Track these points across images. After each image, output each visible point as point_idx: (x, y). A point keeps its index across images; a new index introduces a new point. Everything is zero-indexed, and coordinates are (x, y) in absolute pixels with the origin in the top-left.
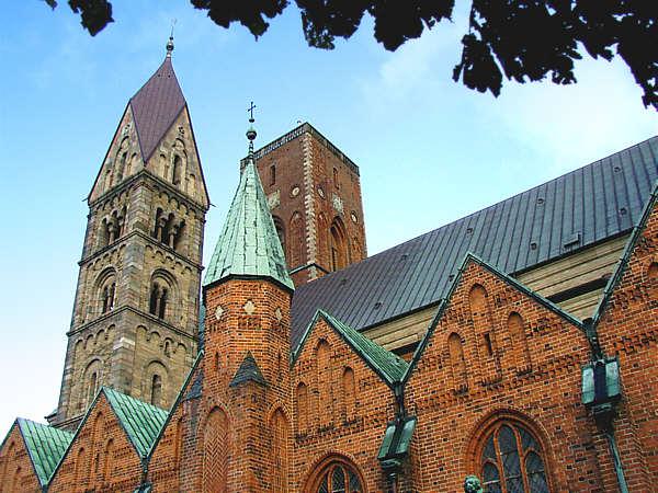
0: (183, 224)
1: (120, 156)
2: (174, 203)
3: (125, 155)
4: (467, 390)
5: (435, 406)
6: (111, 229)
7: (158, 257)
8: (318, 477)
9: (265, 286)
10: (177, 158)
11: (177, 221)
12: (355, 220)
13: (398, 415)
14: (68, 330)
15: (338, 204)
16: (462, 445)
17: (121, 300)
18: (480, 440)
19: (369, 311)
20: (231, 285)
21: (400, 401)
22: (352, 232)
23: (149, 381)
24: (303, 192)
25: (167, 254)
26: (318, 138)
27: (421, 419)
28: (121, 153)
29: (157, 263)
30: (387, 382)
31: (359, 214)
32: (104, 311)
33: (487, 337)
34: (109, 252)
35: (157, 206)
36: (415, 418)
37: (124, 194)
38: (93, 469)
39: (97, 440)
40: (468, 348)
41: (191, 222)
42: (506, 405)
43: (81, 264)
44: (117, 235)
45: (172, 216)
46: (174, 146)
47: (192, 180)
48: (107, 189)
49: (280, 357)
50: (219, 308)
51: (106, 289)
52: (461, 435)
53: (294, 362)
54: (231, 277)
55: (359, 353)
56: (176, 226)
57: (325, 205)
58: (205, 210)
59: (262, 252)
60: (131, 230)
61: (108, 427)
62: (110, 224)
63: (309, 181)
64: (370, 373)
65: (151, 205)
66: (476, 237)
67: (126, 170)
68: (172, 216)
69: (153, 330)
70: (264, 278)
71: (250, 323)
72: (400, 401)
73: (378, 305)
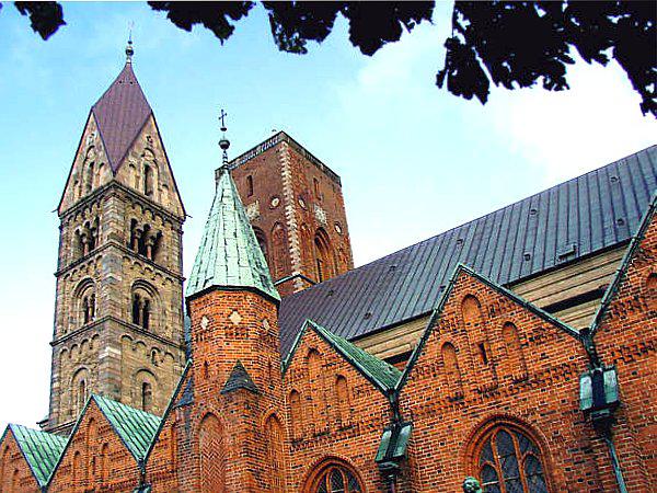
0: (160, 235)
1: (87, 167)
2: (149, 215)
3: (92, 165)
4: (462, 397)
5: (431, 413)
6: (85, 240)
7: (136, 268)
8: (316, 478)
9: (250, 297)
11: (153, 232)
12: (339, 231)
13: (394, 421)
14: (51, 340)
15: (321, 215)
16: (459, 449)
17: (102, 311)
18: (477, 444)
19: (359, 321)
20: (214, 295)
21: (395, 407)
22: (337, 243)
23: (139, 389)
24: (283, 203)
25: (146, 265)
26: (295, 146)
27: (417, 424)
28: (88, 163)
29: (136, 274)
30: (381, 390)
31: (343, 225)
32: (86, 321)
33: (481, 346)
34: (85, 263)
35: (130, 217)
36: (411, 423)
37: (95, 205)
38: (90, 472)
40: (462, 357)
41: (168, 233)
42: (503, 412)
43: (58, 275)
44: (92, 246)
45: (147, 227)
47: (165, 190)
48: (76, 200)
49: (270, 366)
50: (204, 318)
51: (86, 299)
52: (459, 440)
53: (285, 371)
54: (214, 288)
55: (351, 362)
56: (152, 238)
57: (307, 218)
58: (181, 221)
59: (244, 262)
60: (105, 242)
61: (101, 432)
62: (84, 235)
63: (288, 191)
64: (363, 381)
65: (124, 216)
66: (467, 247)
67: (94, 181)
68: (147, 227)
69: (139, 340)
70: (248, 289)
71: (238, 333)
72: (395, 407)
73: (368, 316)
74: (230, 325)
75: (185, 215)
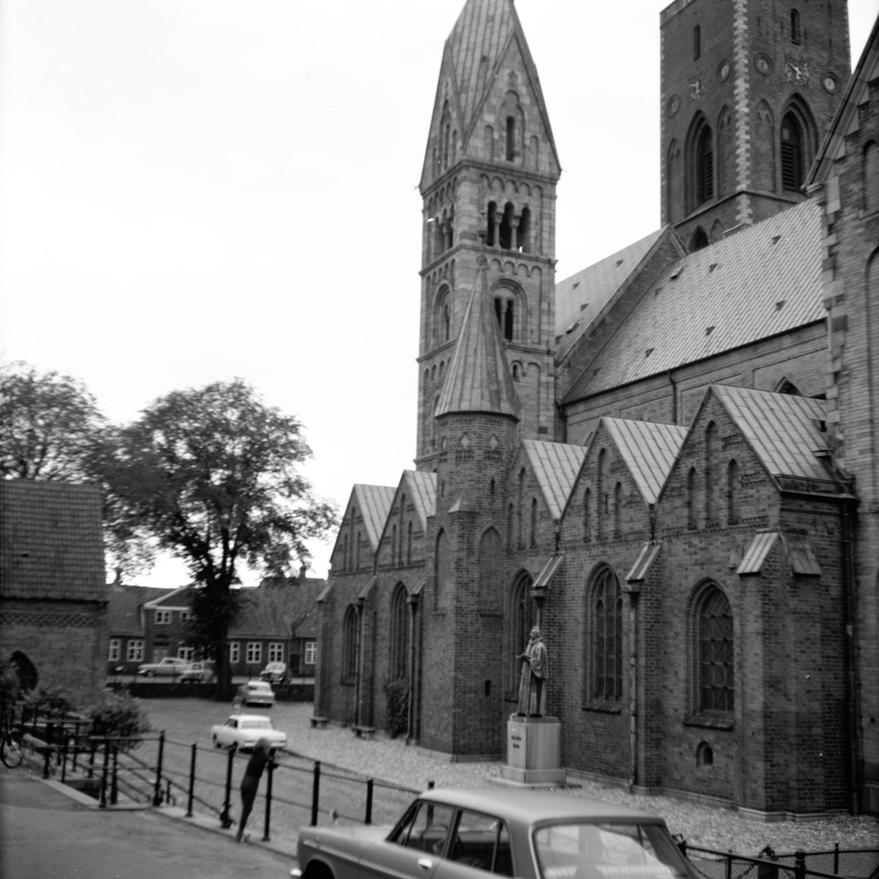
0: (526, 211)
5: (574, 548)
10: (510, 121)
11: (518, 210)
20: (450, 420)
21: (558, 537)
24: (732, 75)
39: (405, 520)
43: (422, 274)
45: (509, 207)
46: (504, 104)
49: (493, 482)
56: (516, 217)
58: (553, 180)
62: (443, 225)
63: (742, 58)
68: (509, 207)
72: (558, 537)
74: (460, 449)
75: (560, 170)
